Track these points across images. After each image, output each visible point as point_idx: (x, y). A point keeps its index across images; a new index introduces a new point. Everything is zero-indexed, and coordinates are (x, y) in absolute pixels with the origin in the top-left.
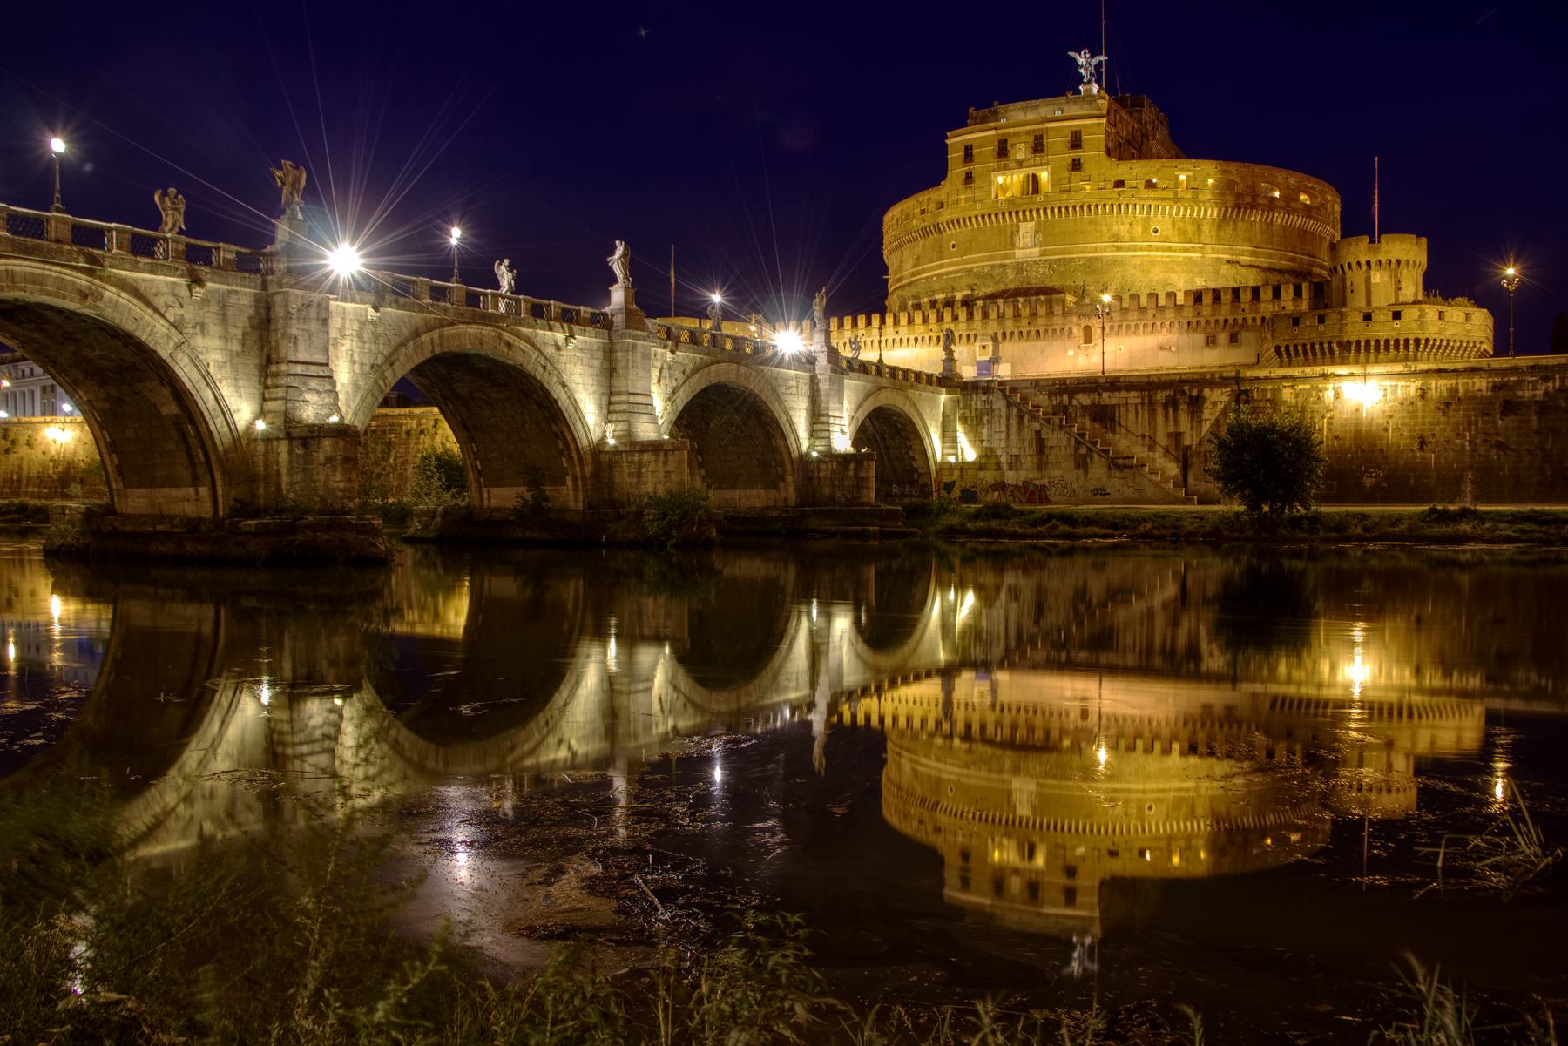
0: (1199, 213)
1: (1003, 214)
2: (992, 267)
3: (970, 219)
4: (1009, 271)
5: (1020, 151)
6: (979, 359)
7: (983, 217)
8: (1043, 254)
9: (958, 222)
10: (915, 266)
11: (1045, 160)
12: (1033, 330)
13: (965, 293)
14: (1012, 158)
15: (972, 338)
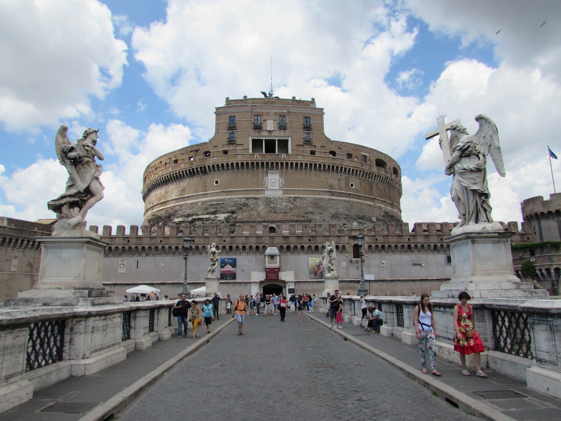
0: (372, 178)
1: (258, 163)
2: (247, 199)
3: (232, 164)
4: (260, 203)
5: (270, 125)
6: (268, 265)
7: (242, 164)
8: (285, 192)
9: (223, 165)
10: (180, 195)
11: (287, 132)
12: (313, 246)
13: (226, 215)
14: (264, 128)
15: (261, 250)
